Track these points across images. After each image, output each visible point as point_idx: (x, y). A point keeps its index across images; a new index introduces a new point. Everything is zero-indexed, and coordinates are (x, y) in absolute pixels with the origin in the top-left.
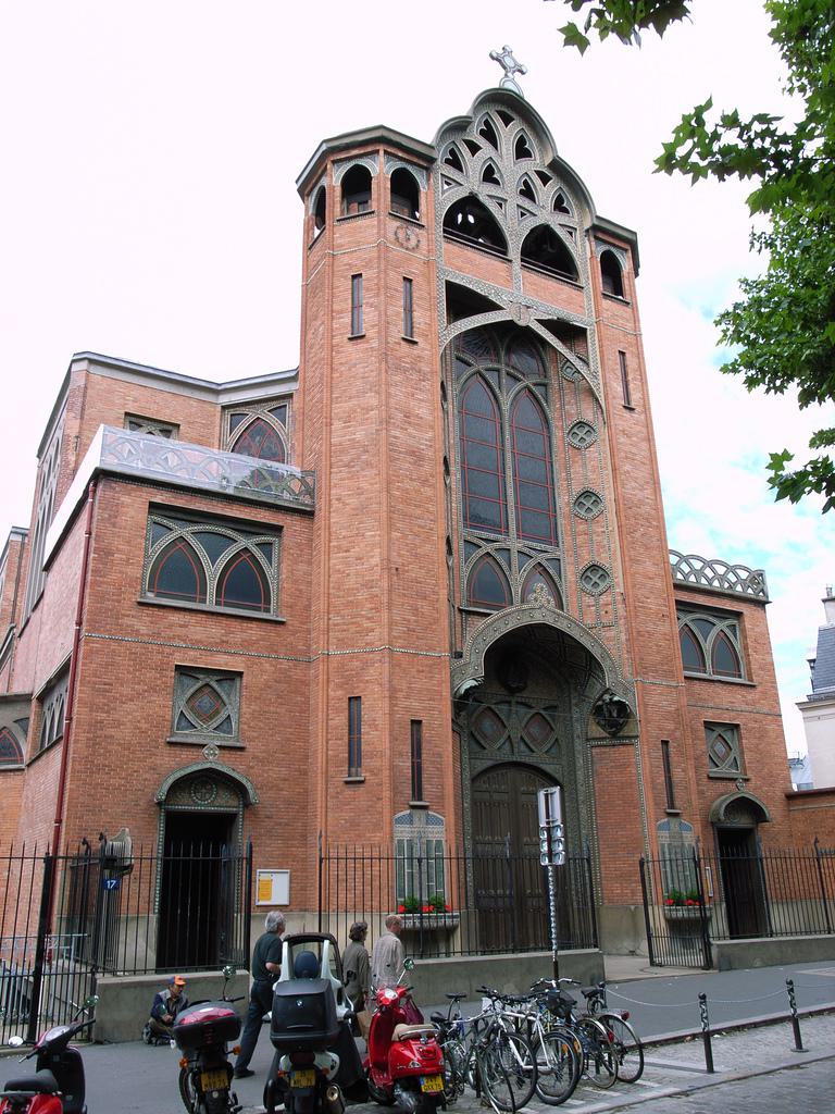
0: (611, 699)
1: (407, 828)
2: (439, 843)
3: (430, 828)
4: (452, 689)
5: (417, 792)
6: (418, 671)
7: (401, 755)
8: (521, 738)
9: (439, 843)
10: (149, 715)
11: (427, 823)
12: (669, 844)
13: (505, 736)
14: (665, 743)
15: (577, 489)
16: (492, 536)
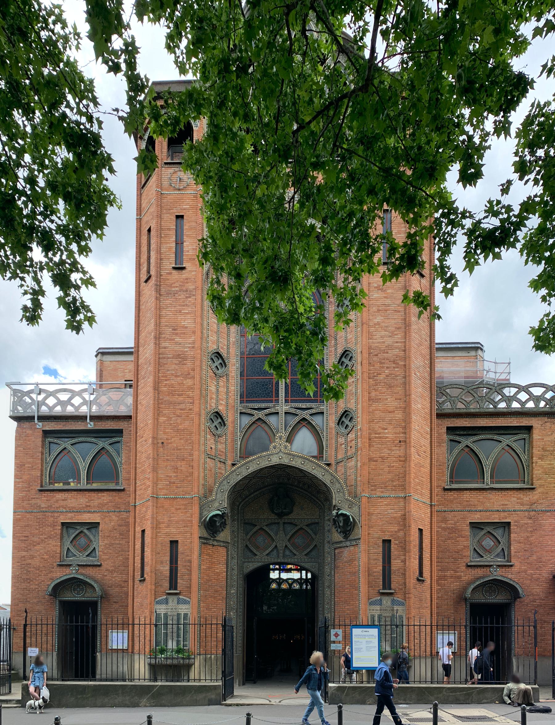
0: (337, 513)
1: (163, 606)
2: (186, 615)
3: (181, 606)
4: (201, 519)
5: (173, 584)
6: (177, 509)
7: (162, 562)
8: (286, 546)
9: (186, 615)
10: (48, 551)
11: (178, 603)
12: (379, 616)
13: (273, 546)
14: (387, 543)
15: (340, 351)
16: (263, 405)
